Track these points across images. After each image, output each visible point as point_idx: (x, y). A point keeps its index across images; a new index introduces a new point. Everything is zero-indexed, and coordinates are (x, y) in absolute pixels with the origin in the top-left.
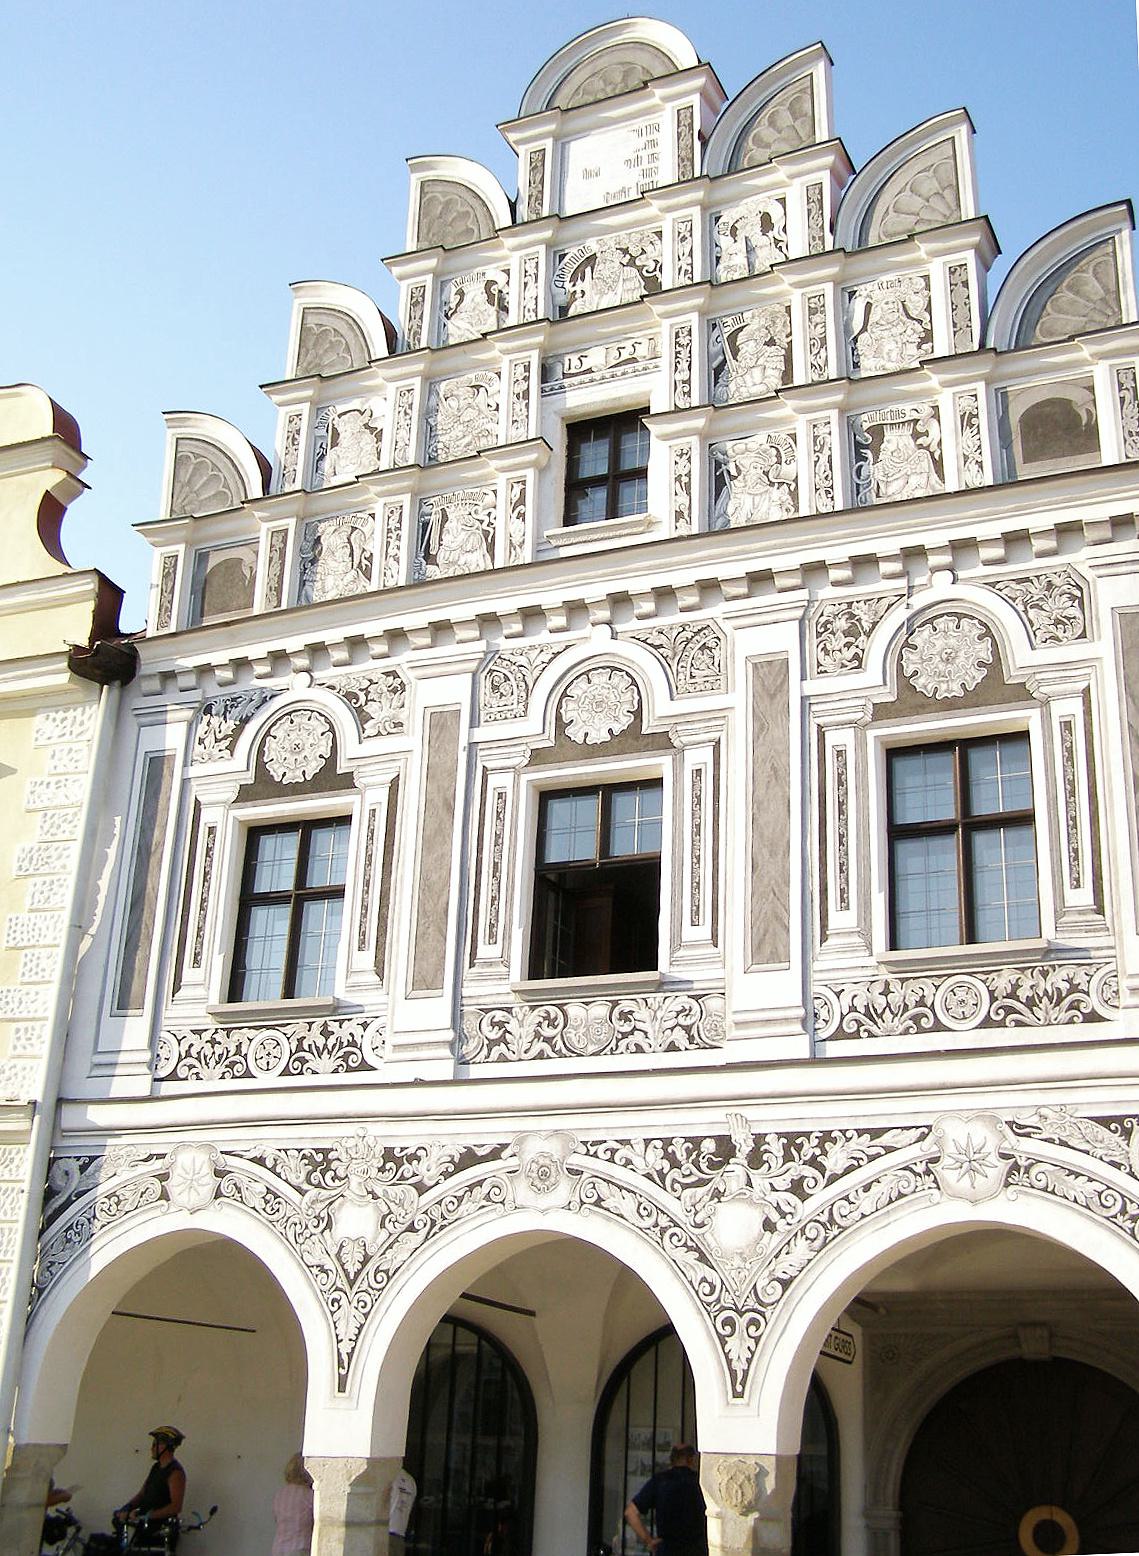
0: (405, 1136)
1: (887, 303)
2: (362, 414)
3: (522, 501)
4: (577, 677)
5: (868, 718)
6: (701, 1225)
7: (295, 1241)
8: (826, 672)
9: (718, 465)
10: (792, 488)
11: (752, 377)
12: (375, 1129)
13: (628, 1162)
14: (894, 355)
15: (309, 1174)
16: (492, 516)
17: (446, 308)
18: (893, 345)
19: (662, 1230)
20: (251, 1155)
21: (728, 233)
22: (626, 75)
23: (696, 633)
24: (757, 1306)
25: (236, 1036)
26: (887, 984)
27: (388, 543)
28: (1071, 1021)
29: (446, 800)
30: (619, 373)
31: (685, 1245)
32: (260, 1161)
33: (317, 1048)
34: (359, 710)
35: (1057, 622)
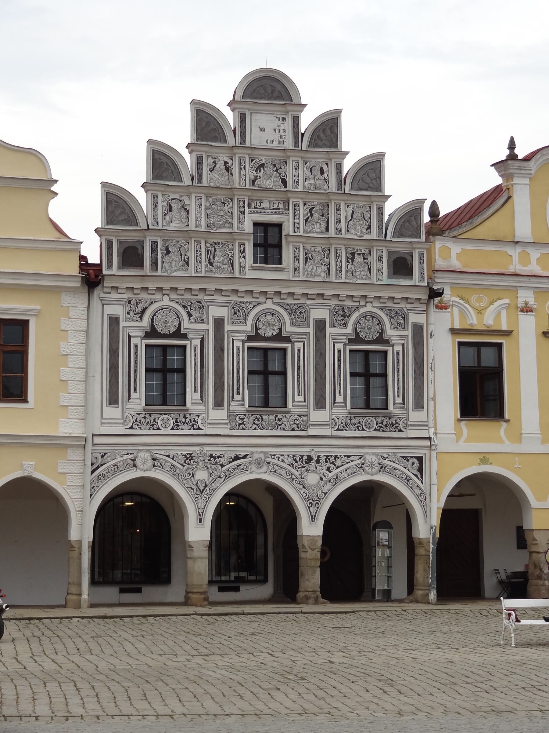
0: (216, 451)
1: (358, 213)
2: (181, 201)
3: (244, 252)
4: (262, 315)
5: (347, 342)
6: (303, 478)
7: (182, 480)
8: (336, 326)
9: (306, 254)
10: (328, 267)
11: (317, 226)
12: (206, 448)
13: (283, 461)
14: (359, 231)
15: (185, 461)
16: (232, 253)
17: (209, 167)
18: (359, 227)
19: (292, 479)
20: (166, 454)
21: (309, 170)
22: (273, 91)
23: (299, 307)
24: (318, 499)
25: (153, 416)
26: (351, 417)
27: (197, 256)
28: (395, 431)
29: (221, 348)
30: (274, 212)
31: (299, 483)
32: (168, 456)
33: (183, 422)
34: (188, 312)
35: (398, 323)
